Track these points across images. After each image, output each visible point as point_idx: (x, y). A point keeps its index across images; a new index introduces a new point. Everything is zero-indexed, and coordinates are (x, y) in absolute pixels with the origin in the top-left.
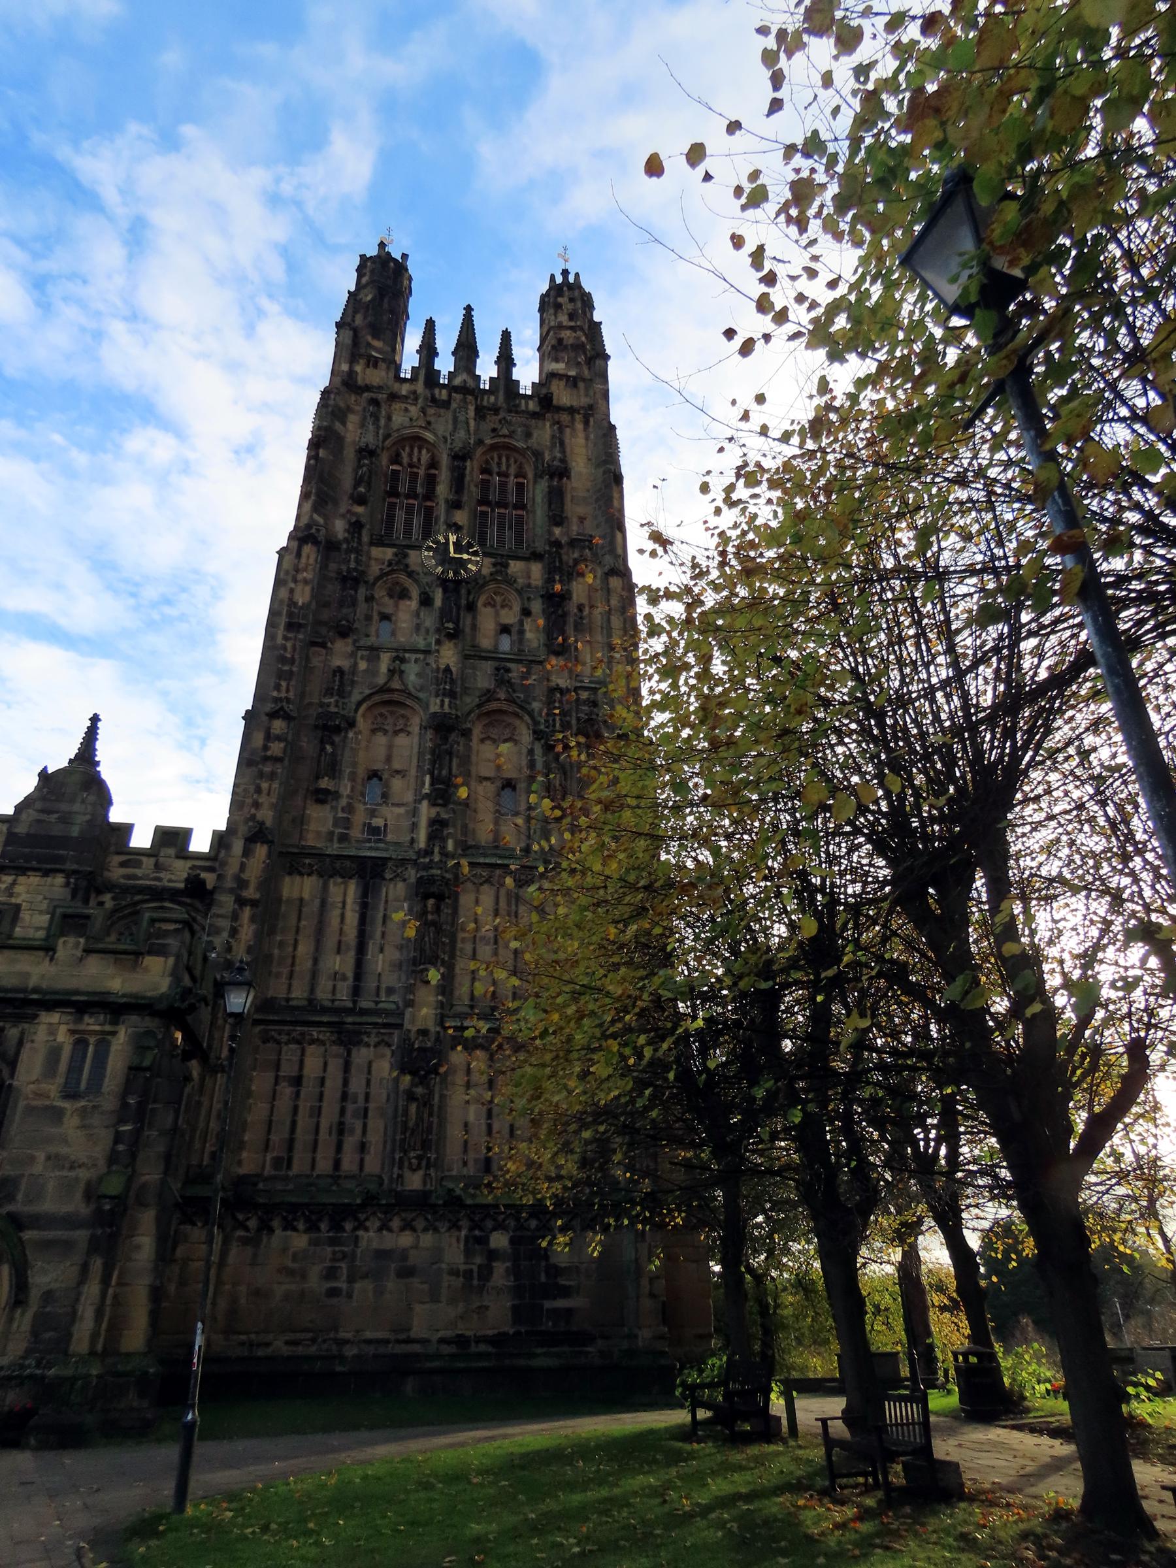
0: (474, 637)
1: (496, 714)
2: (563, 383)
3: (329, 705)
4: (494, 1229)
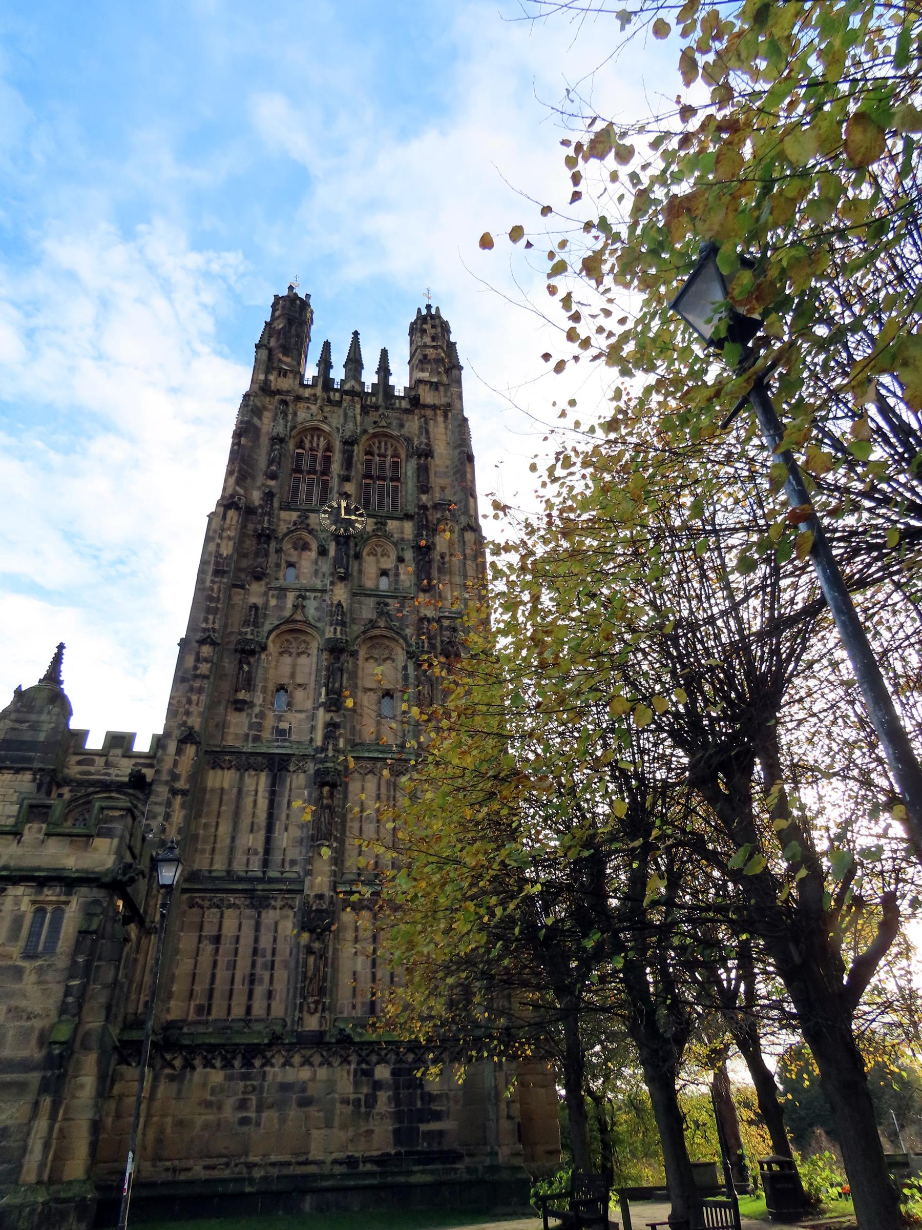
0: (360, 579)
1: (378, 637)
2: (427, 388)
3: (246, 633)
4: (378, 1063)
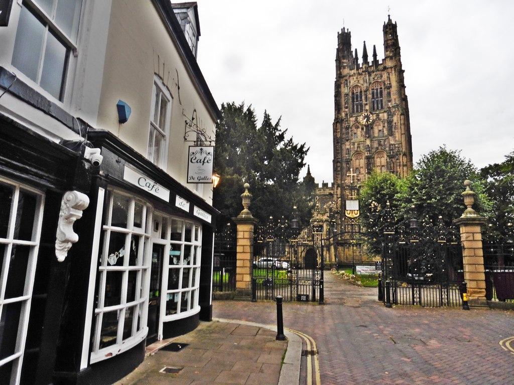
1: (379, 152)
2: (389, 59)
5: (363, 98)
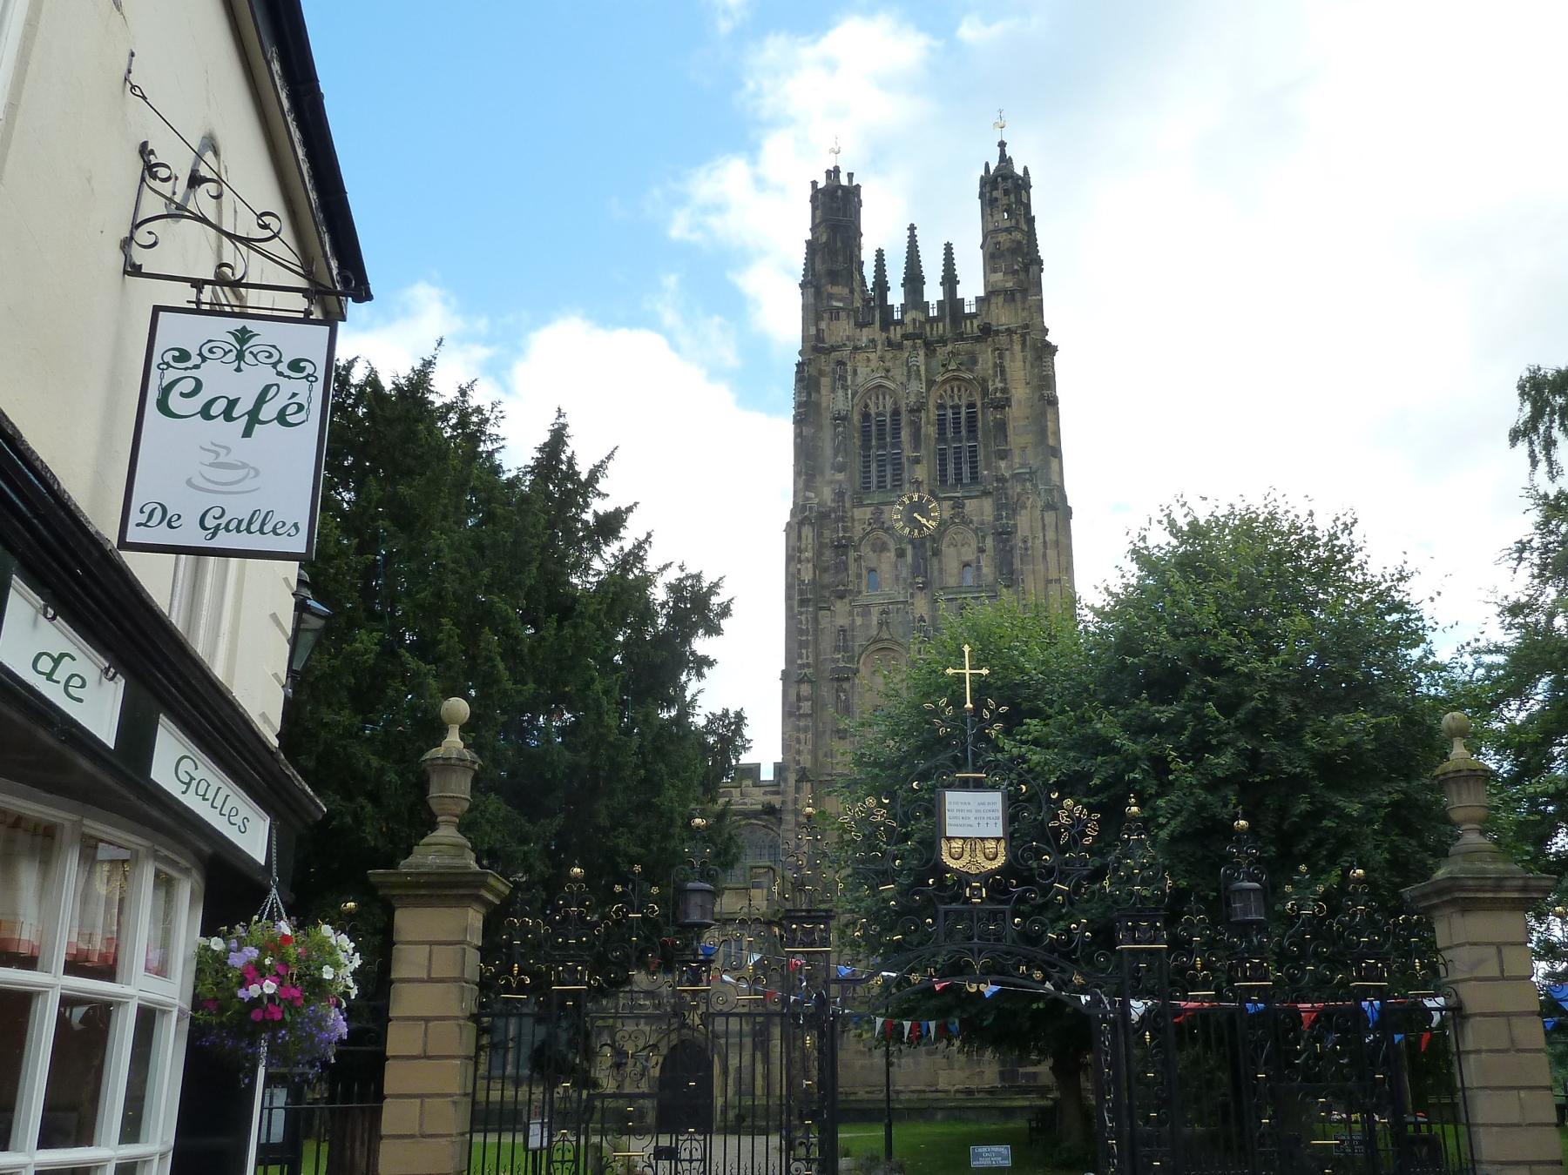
2: (1000, 299)
5: (905, 434)
